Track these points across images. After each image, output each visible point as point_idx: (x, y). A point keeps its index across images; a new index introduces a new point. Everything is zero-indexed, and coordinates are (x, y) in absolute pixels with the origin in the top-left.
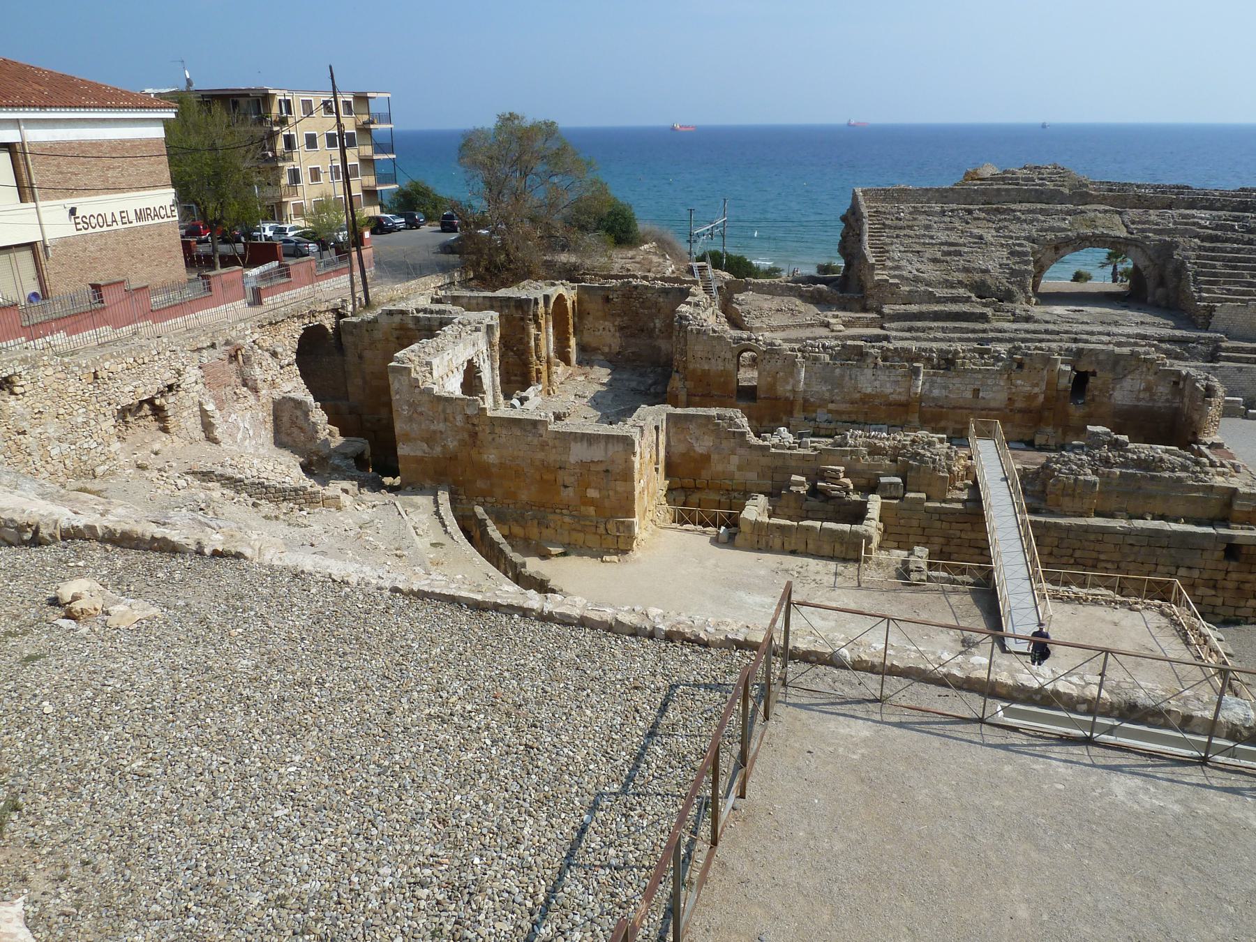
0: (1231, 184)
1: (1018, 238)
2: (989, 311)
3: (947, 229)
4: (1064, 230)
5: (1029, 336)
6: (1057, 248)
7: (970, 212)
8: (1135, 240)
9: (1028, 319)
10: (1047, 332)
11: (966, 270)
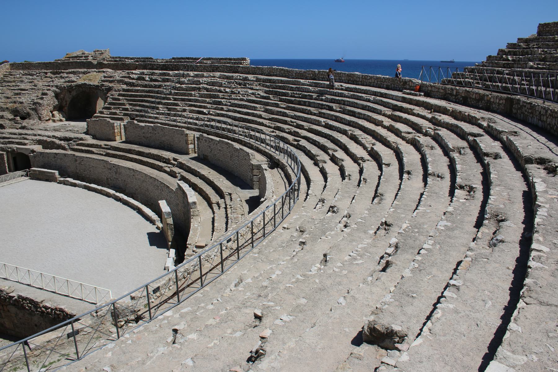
0: (168, 57)
1: (52, 86)
2: (6, 123)
3: (30, 82)
4: (73, 82)
5: (11, 136)
6: (70, 92)
7: (46, 73)
8: (97, 86)
9: (23, 128)
10: (20, 134)
11: (15, 102)
